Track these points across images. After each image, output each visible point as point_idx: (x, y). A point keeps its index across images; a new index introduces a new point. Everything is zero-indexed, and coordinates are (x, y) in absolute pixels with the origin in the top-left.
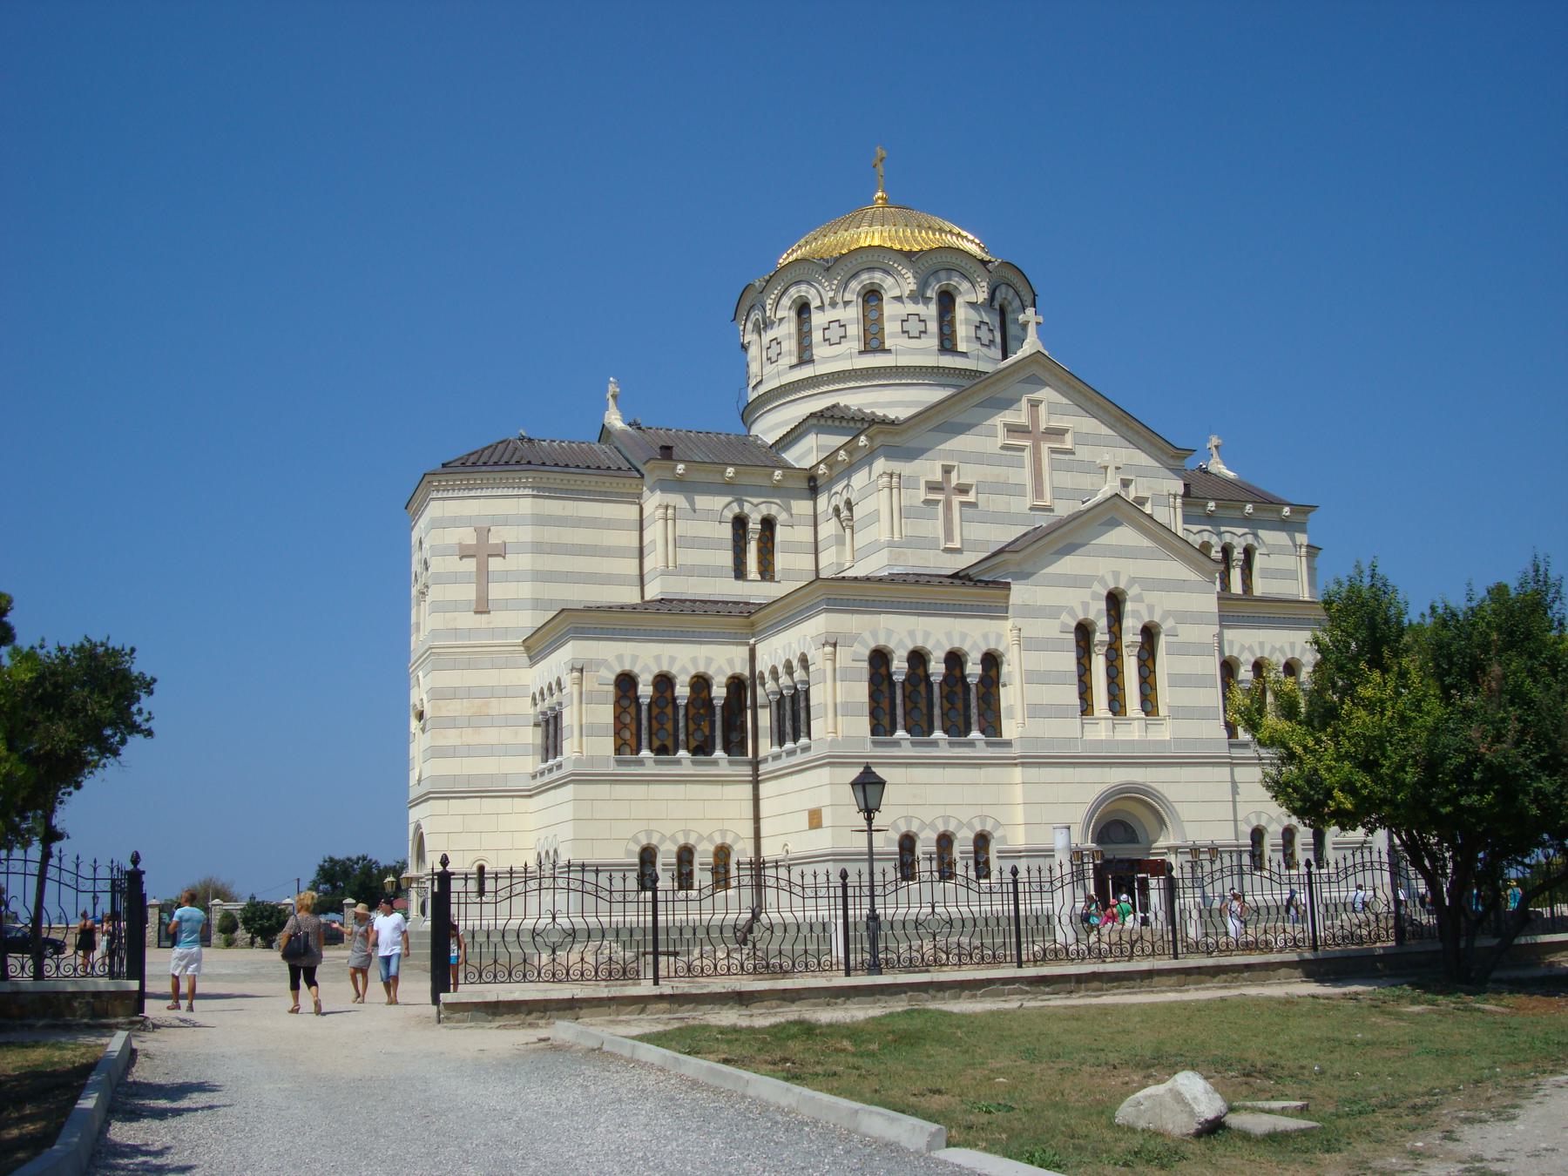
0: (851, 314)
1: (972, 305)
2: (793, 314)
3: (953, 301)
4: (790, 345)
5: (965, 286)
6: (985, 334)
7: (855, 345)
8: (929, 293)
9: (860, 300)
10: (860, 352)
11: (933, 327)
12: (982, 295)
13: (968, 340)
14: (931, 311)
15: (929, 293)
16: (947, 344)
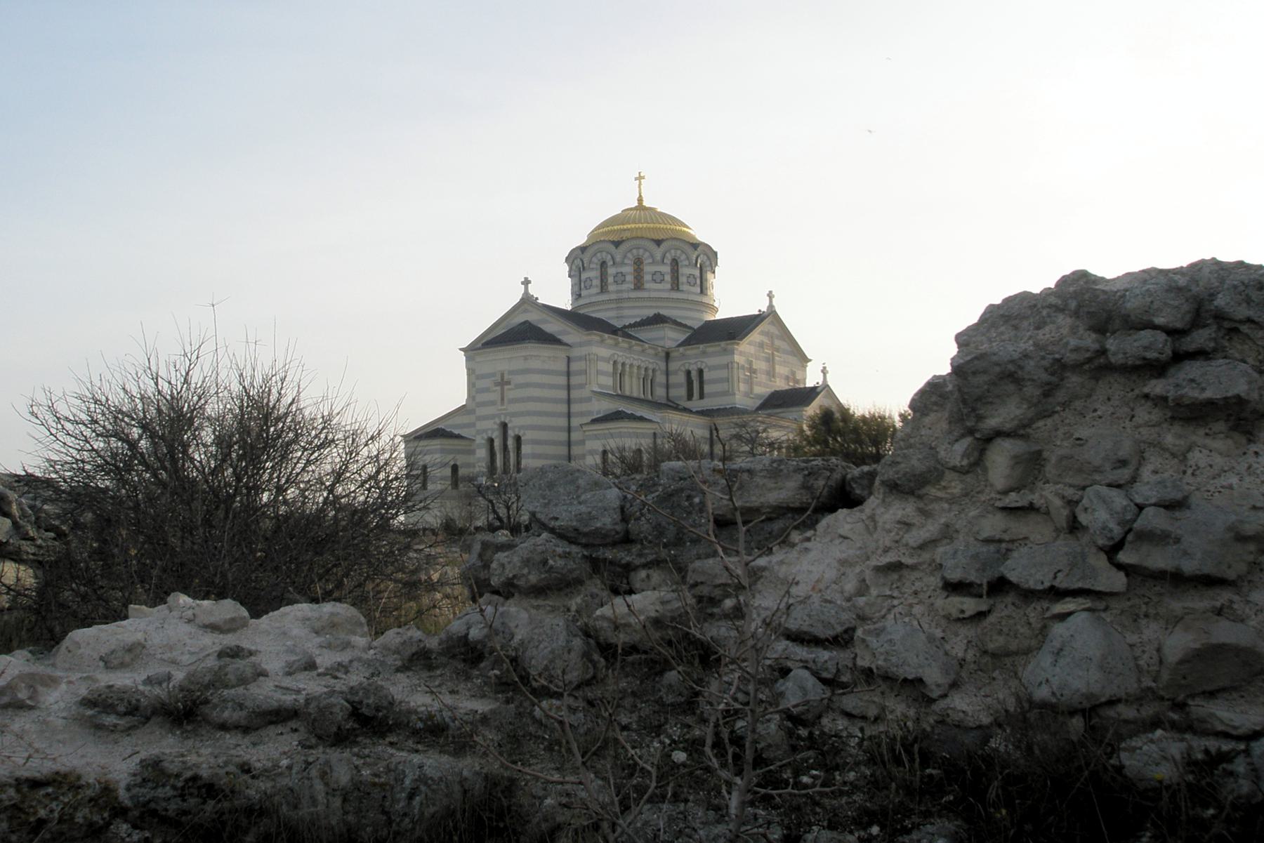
0: (594, 274)
1: (654, 263)
2: (577, 273)
3: (642, 263)
4: (577, 288)
5: (647, 254)
6: (658, 277)
7: (594, 290)
8: (626, 261)
9: (599, 267)
10: (598, 294)
11: (630, 278)
12: (658, 257)
13: (648, 282)
14: (628, 269)
15: (626, 261)
16: (639, 285)
